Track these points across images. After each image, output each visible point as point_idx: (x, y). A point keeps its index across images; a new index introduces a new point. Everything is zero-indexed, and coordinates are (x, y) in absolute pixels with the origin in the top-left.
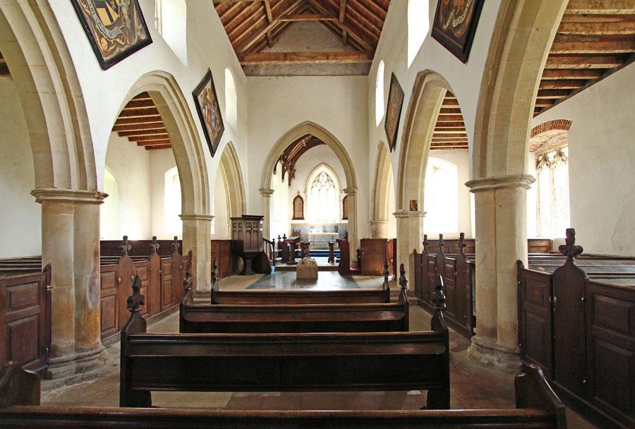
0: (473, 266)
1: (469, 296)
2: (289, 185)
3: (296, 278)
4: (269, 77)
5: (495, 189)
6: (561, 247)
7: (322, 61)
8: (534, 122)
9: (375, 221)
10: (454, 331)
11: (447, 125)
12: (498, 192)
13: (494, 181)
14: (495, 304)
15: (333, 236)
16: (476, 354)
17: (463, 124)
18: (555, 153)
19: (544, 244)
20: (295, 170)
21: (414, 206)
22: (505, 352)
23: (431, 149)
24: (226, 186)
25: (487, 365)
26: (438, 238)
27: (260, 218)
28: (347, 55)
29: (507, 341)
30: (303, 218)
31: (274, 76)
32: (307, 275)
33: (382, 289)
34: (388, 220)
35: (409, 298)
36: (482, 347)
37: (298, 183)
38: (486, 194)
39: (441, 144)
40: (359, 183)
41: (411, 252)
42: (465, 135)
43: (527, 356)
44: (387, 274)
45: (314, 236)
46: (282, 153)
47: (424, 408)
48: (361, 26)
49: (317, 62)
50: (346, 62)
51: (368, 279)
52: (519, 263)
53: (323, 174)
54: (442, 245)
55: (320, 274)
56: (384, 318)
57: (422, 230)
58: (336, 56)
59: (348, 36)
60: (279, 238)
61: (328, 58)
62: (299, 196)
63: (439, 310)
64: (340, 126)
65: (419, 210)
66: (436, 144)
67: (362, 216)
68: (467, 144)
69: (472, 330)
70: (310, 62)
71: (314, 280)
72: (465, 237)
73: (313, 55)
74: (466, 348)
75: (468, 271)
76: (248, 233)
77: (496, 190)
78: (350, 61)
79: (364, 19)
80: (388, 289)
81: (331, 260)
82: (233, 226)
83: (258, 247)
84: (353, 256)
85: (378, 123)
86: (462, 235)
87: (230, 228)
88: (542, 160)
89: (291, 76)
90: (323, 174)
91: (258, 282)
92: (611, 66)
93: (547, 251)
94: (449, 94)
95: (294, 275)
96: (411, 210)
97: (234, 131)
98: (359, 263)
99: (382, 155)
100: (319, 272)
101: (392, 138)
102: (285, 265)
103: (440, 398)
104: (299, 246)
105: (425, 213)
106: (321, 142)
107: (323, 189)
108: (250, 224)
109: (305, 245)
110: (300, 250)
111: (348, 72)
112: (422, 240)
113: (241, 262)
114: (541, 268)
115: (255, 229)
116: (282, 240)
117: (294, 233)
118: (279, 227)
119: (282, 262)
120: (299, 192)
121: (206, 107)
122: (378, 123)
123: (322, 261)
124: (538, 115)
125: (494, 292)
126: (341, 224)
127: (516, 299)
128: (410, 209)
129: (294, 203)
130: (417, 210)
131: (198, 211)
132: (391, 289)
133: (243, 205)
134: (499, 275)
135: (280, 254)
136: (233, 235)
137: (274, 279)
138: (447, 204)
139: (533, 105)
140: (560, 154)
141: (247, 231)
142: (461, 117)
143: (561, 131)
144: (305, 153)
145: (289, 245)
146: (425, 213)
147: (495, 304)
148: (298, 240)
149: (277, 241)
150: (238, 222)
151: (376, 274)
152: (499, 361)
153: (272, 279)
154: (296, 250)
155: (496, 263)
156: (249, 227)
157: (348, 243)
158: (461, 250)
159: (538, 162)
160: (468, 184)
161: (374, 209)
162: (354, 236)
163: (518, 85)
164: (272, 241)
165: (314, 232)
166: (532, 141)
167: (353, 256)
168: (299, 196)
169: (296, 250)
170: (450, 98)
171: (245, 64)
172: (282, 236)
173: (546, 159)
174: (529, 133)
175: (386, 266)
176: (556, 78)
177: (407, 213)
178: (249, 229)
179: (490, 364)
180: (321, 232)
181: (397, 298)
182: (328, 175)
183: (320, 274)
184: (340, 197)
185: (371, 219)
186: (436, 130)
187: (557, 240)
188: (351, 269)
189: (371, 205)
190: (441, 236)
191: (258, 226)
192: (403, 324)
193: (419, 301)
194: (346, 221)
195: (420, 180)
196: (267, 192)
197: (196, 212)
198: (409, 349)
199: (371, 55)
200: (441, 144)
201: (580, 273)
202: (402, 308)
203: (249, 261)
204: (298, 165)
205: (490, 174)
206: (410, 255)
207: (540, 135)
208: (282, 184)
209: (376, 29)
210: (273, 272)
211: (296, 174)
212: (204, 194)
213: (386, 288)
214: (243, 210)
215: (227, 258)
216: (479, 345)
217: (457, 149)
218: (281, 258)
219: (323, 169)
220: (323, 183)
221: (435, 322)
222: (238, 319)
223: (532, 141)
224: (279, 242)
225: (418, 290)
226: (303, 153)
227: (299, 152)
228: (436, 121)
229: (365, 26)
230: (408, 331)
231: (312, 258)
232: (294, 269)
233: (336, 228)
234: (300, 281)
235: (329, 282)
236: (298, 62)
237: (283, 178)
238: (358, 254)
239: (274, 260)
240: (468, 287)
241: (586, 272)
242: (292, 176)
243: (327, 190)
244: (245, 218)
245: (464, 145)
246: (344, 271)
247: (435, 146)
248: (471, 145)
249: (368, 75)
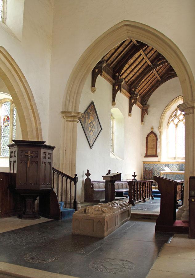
2: (142, 120)
30: (156, 156)
37: (152, 119)
62: (152, 132)
120: (152, 128)
129: (147, 140)
168: (152, 132)
211: (149, 109)
226: (157, 87)
242: (145, 111)
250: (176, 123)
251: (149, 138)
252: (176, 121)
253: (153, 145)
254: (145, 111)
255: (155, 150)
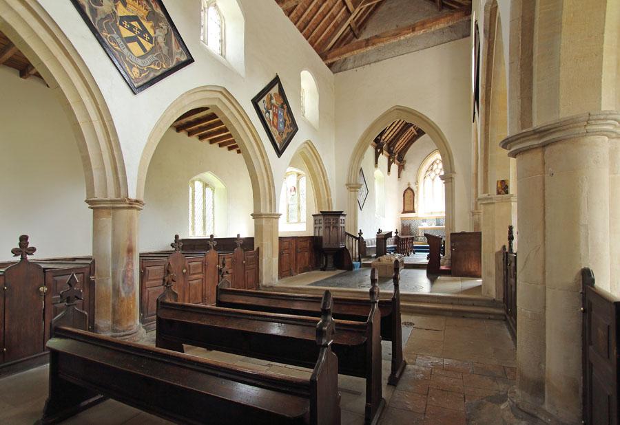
2: (399, 177)
30: (413, 211)
37: (408, 174)
97: (316, 130)
120: (409, 184)
121: (271, 111)
131: (265, 209)
133: (329, 201)
165: (425, 225)
180: (434, 226)
197: (262, 211)
204: (408, 155)
211: (405, 165)
212: (270, 193)
215: (306, 253)
227: (409, 141)
242: (401, 168)
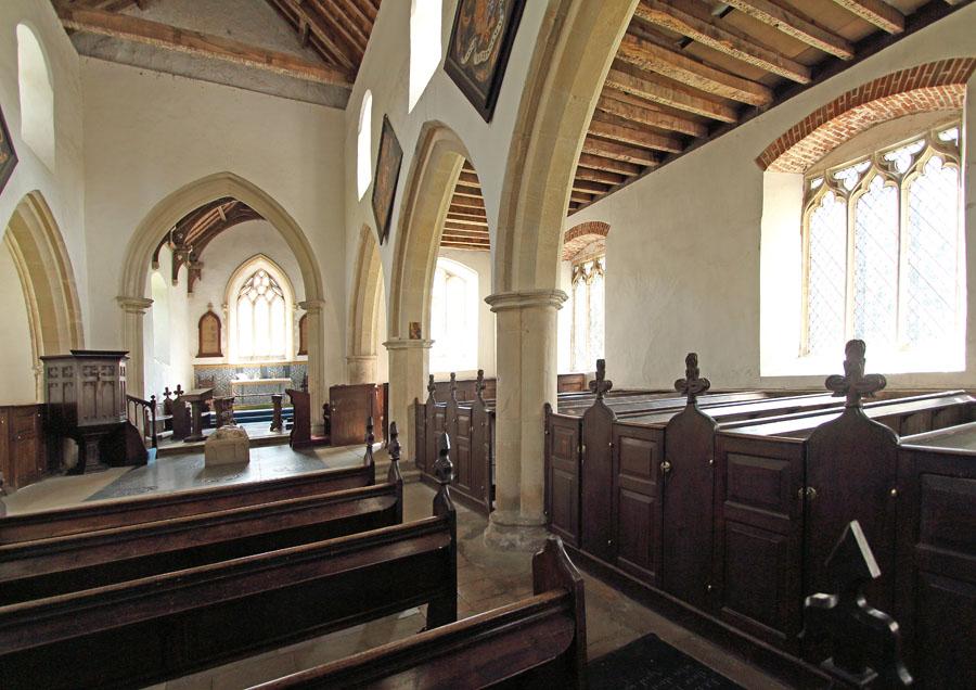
0: (493, 415)
1: (487, 458)
2: (190, 290)
3: (203, 465)
4: (140, 70)
5: (522, 307)
6: (592, 383)
7: (260, 65)
8: (569, 223)
9: (355, 356)
10: (467, 510)
11: (466, 211)
12: (525, 311)
13: (521, 296)
14: (519, 466)
15: (280, 385)
16: (495, 535)
17: (483, 212)
18: (591, 264)
19: (577, 380)
20: (201, 264)
21: (416, 331)
22: (530, 526)
23: (443, 244)
24: (25, 288)
25: (507, 549)
26: (449, 379)
27: (119, 356)
28: (307, 65)
29: (533, 511)
31: (151, 69)
32: (227, 457)
33: (362, 465)
34: (375, 354)
35: (402, 474)
36: (502, 524)
37: (209, 290)
38: (511, 313)
39: (457, 239)
40: (327, 293)
41: (410, 402)
42: (486, 229)
43: (553, 525)
44: (371, 440)
45: (243, 386)
46: (171, 227)
47: (423, 630)
48: (333, 21)
49: (248, 63)
50: (306, 77)
51: (344, 451)
52: (547, 406)
53: (262, 274)
54: (454, 389)
55: (253, 452)
56: (365, 510)
57: (428, 370)
58: (285, 61)
59: (310, 31)
60: (167, 393)
61: (269, 62)
62: (210, 313)
63: (444, 485)
64: (293, 193)
65: (423, 337)
66: (451, 239)
67: (331, 348)
68: (488, 242)
69: (491, 504)
70: (231, 59)
71: (242, 465)
72: (485, 376)
73: (240, 49)
74: (482, 532)
75: (487, 424)
76: (89, 391)
77: (521, 308)
78: (312, 78)
79: (339, 10)
80: (373, 463)
81: (277, 426)
82: (49, 373)
83: (115, 414)
84: (316, 416)
85: (361, 196)
86: (480, 373)
87: (41, 378)
88: (578, 273)
89: (190, 77)
90: (262, 274)
91: (115, 483)
92: (676, 152)
93: (580, 390)
94: (467, 165)
95: (200, 461)
96: (411, 337)
98: (327, 427)
99: (367, 248)
100: (251, 450)
101: (383, 223)
102: (181, 444)
103: (443, 609)
104: (212, 407)
105: (433, 342)
106: (257, 216)
107: (262, 302)
108: (95, 368)
109: (224, 405)
110: (213, 413)
111: (310, 97)
112: (426, 382)
113: (72, 449)
114: (570, 411)
115: (108, 378)
116: (173, 397)
117: (200, 382)
118: (167, 370)
119: (173, 438)
120: (210, 305)
122: (361, 196)
123: (262, 430)
124: (574, 212)
125: (517, 449)
126: (295, 363)
127: (543, 457)
128: (410, 335)
130: (419, 337)
132: (376, 463)
134: (524, 426)
135: (169, 425)
136: (48, 393)
137: (155, 473)
138: (460, 335)
139: (568, 198)
140: (597, 266)
141: (85, 384)
142: (481, 202)
143: (599, 236)
144: (219, 235)
145: (188, 405)
146: (433, 342)
147: (519, 466)
148: (209, 395)
149: (161, 399)
150: (60, 364)
151: (353, 442)
152: (522, 540)
153: (150, 474)
154: (204, 414)
155: (520, 409)
156: (92, 374)
157: (309, 395)
158: (479, 394)
159: (574, 275)
160: (489, 300)
161: (354, 337)
162: (318, 382)
163: (552, 168)
164: (148, 399)
165: (243, 378)
166: (566, 247)
167: (316, 416)
169: (204, 414)
170: (468, 173)
171: (76, 26)
172: (173, 389)
173: (582, 271)
174: (562, 237)
175: (370, 428)
176: (596, 168)
177: (405, 343)
178: (91, 379)
179: (512, 545)
180: (257, 379)
181: (386, 476)
182: (270, 277)
183: (253, 452)
184: (294, 315)
185: (348, 353)
186: (449, 217)
187: (590, 375)
188: (313, 438)
189: (349, 329)
190: (453, 375)
191: (114, 371)
192: (394, 514)
193: (421, 476)
194: (305, 358)
195: (425, 291)
196: (136, 304)
198: (404, 549)
199: (351, 76)
200: (457, 239)
201: (608, 412)
202: (394, 489)
203: (93, 445)
204: (204, 255)
205: (516, 288)
206: (409, 408)
207: (577, 239)
208: (174, 288)
209: (360, 33)
210: (152, 461)
213: (369, 463)
214: (75, 340)
215: (32, 442)
216: (498, 523)
217: (478, 249)
218: (171, 432)
219: (261, 264)
220: (262, 290)
221: (439, 503)
222: (58, 566)
223: (566, 247)
224: (168, 403)
225: (421, 459)
226: (219, 231)
227: (210, 229)
228: (449, 203)
229: (340, 21)
230: (401, 522)
231: (238, 425)
232: (201, 449)
233: (287, 370)
234: (213, 469)
235: (270, 465)
236: (207, 55)
237: (175, 277)
238: (325, 413)
239: (154, 438)
240: (487, 445)
241: (614, 411)
242: (195, 274)
243: (270, 303)
244: (79, 355)
245: (484, 243)
246: (300, 442)
247: (448, 241)
248: (493, 244)
249: (344, 109)
250: (253, 299)
251: (204, 322)
252: (253, 294)
253: (214, 336)
254: (195, 274)
255: (217, 344)
